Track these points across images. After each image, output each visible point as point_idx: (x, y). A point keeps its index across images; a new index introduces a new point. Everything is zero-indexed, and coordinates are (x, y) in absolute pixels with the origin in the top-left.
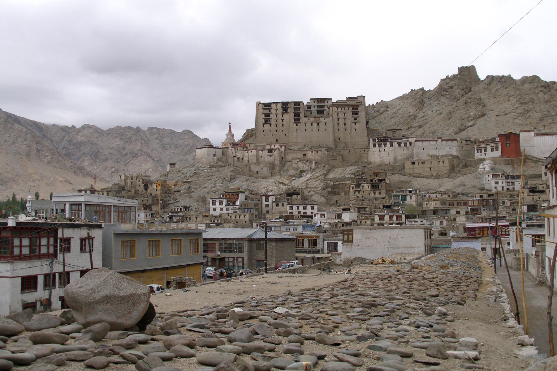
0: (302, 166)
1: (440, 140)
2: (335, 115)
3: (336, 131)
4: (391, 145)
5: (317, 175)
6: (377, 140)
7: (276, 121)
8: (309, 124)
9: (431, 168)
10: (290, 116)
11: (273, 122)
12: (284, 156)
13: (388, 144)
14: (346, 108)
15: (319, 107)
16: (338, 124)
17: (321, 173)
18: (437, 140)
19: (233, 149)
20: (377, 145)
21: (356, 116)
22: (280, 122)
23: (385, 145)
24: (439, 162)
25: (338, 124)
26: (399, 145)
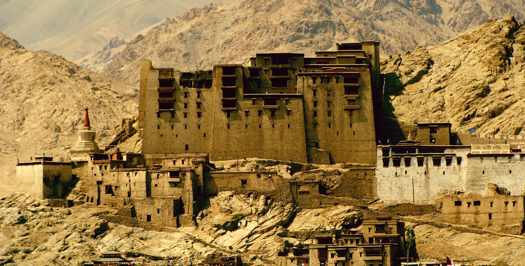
0: (239, 204)
1: (517, 156)
4: (420, 163)
5: (269, 224)
8: (254, 113)
9: (490, 216)
13: (414, 161)
17: (277, 220)
18: (513, 155)
20: (391, 162)
21: (353, 96)
22: (193, 109)
23: (408, 163)
24: (506, 203)
26: (437, 162)
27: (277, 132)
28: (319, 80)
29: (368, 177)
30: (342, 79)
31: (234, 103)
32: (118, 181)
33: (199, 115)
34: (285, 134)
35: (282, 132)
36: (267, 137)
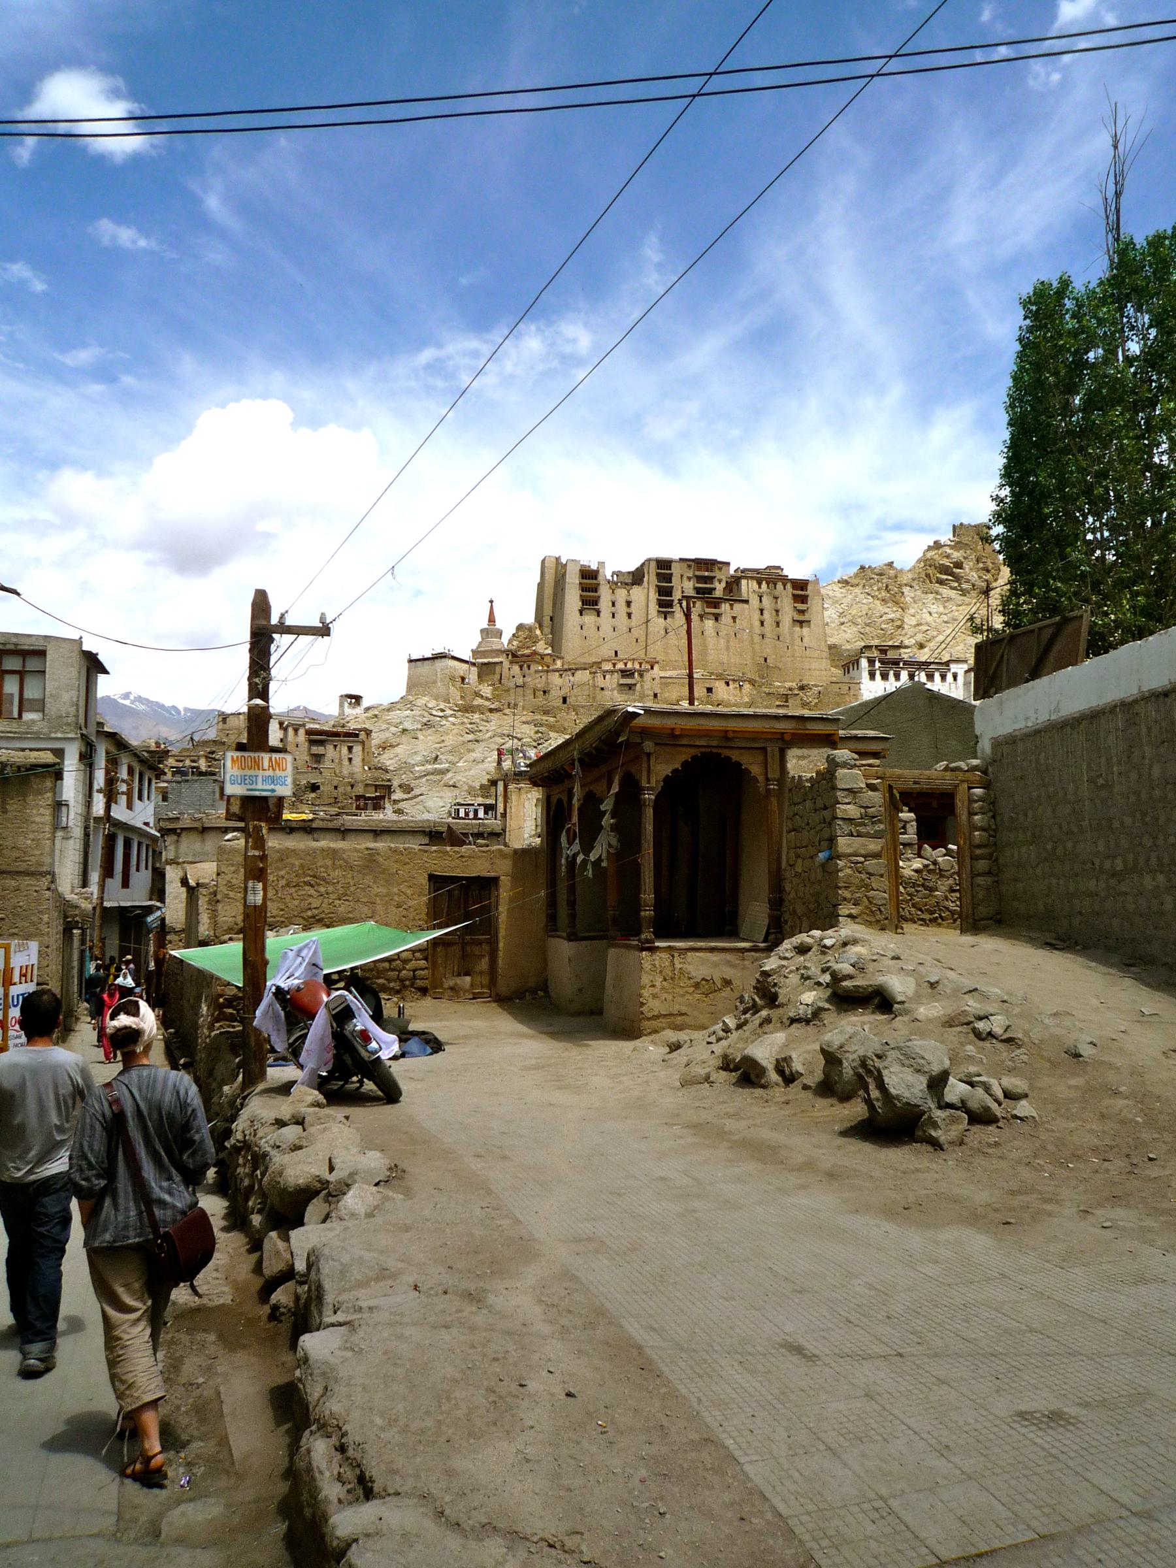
2: (754, 601)
3: (757, 639)
6: (877, 665)
7: (613, 604)
10: (645, 596)
11: (604, 605)
12: (658, 691)
14: (780, 585)
15: (700, 579)
16: (762, 623)
19: (516, 668)
22: (621, 608)
25: (762, 623)
27: (722, 641)
28: (764, 585)
29: (852, 692)
30: (789, 586)
31: (670, 604)
32: (547, 683)
33: (629, 615)
34: (732, 644)
35: (728, 641)
36: (711, 646)
